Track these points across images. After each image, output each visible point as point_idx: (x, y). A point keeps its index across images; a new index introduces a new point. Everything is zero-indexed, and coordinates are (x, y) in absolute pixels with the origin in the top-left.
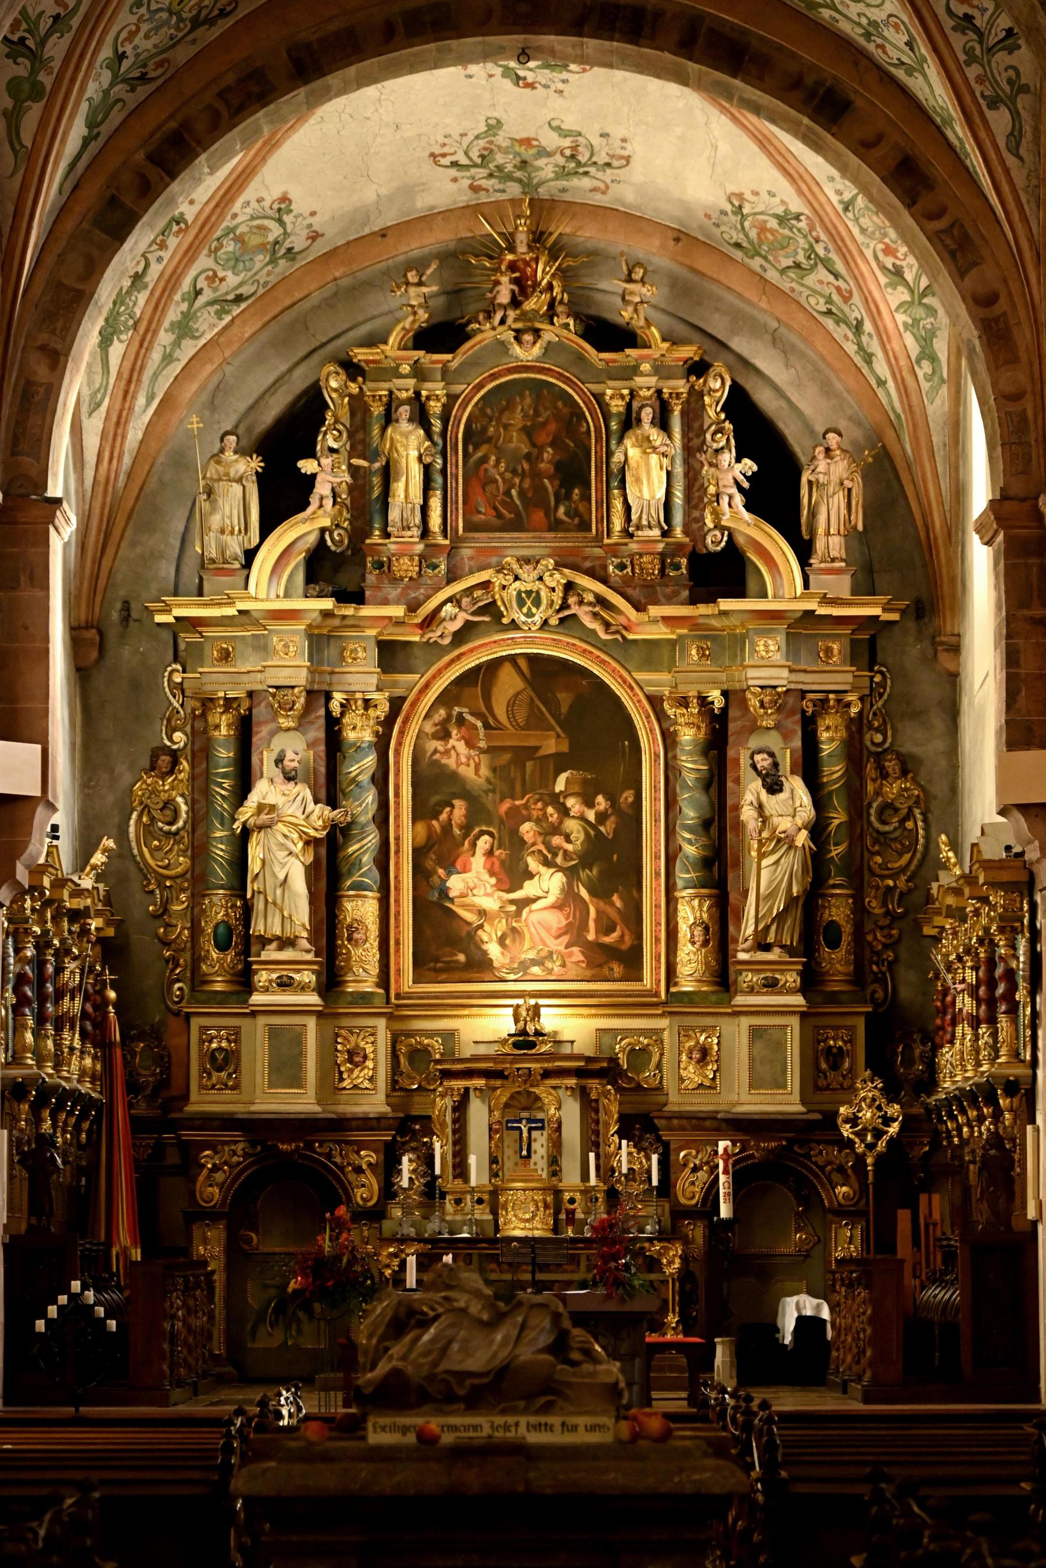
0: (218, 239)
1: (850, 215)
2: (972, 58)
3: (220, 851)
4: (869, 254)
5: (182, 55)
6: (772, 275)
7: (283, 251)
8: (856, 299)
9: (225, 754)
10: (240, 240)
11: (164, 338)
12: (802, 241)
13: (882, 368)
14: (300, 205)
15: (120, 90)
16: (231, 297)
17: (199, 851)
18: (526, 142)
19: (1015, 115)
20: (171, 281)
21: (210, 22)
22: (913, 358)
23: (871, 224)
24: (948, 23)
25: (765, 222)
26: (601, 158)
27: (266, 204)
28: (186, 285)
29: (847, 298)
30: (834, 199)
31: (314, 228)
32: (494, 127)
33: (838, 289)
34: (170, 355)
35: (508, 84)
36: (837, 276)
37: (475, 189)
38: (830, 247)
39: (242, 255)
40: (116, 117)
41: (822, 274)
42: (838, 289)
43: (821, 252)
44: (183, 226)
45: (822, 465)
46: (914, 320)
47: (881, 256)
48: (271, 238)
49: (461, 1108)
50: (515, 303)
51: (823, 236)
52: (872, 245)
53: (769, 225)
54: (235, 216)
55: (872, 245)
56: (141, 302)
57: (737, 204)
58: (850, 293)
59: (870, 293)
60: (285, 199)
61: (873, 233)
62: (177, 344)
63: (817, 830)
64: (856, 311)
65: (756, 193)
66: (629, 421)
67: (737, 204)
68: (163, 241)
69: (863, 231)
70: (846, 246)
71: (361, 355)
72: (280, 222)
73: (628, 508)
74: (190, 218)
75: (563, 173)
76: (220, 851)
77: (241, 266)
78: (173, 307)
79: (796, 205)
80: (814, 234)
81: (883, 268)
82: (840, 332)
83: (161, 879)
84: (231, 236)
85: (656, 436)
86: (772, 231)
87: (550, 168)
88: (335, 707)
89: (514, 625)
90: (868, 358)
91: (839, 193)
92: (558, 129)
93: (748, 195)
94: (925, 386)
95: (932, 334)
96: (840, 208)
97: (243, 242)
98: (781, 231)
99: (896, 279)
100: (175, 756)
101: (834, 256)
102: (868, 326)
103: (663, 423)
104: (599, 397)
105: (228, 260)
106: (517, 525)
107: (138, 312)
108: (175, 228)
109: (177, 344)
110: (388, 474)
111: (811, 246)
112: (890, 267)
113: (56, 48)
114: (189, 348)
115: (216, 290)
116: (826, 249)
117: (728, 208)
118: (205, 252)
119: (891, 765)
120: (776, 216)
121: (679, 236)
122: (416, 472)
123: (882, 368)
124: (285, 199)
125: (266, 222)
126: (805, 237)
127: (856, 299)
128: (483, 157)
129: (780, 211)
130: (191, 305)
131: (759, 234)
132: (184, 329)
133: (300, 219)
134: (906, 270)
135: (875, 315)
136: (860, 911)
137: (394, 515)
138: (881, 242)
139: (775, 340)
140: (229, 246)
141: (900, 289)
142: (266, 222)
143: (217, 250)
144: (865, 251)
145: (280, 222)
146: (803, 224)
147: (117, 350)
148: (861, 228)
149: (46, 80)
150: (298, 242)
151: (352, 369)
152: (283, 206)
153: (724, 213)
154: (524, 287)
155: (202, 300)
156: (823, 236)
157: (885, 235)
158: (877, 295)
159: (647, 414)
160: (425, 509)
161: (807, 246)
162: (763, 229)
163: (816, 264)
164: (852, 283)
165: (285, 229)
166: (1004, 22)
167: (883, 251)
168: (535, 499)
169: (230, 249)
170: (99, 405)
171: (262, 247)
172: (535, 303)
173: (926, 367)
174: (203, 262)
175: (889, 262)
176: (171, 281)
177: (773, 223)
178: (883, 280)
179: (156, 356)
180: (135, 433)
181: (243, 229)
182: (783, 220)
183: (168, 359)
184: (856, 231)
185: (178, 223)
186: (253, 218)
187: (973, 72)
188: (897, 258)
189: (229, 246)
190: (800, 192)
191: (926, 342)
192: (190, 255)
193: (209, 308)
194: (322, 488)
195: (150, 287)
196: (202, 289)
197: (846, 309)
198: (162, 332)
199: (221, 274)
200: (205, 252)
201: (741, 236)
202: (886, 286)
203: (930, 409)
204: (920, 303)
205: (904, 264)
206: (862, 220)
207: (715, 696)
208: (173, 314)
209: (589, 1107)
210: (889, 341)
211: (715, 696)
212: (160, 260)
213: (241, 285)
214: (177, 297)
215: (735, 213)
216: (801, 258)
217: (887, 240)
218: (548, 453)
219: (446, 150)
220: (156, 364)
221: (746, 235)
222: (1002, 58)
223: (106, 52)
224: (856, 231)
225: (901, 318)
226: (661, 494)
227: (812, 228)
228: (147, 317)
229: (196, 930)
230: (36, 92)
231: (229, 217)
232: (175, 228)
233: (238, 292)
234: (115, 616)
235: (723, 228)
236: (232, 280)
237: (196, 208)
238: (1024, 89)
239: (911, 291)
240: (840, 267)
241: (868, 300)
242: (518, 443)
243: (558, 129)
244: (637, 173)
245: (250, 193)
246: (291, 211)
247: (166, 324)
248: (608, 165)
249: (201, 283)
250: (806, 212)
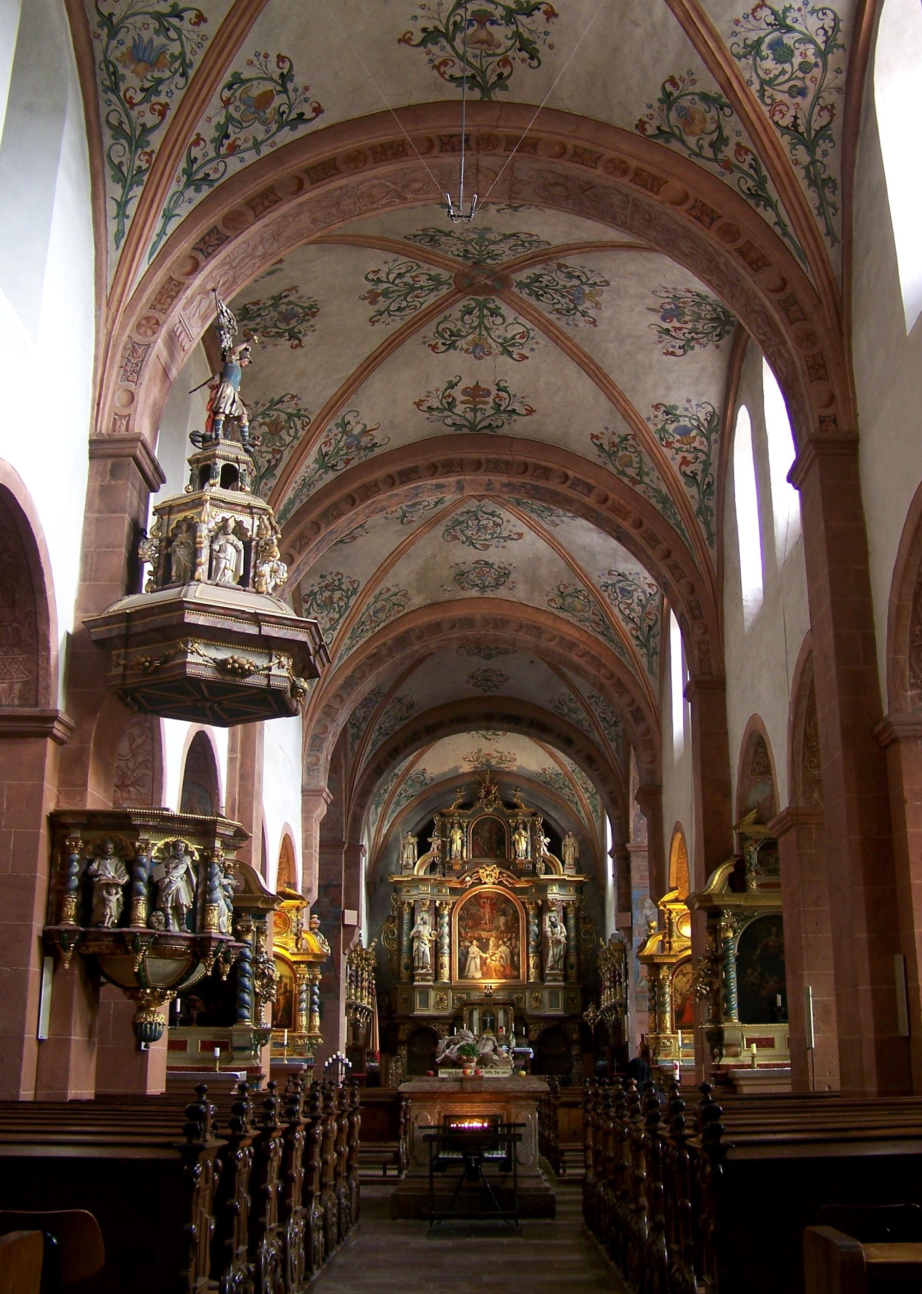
2: (606, 729)
3: (405, 943)
5: (397, 728)
6: (553, 790)
9: (406, 917)
10: (413, 780)
11: (392, 806)
13: (583, 815)
14: (429, 771)
15: (381, 737)
17: (400, 943)
18: (488, 755)
19: (617, 744)
20: (394, 792)
21: (405, 719)
24: (599, 719)
28: (398, 792)
29: (573, 796)
32: (480, 751)
40: (380, 744)
45: (567, 840)
49: (471, 1014)
50: (486, 797)
62: (395, 808)
63: (567, 938)
64: (576, 799)
66: (516, 828)
71: (444, 810)
73: (516, 851)
75: (498, 763)
76: (405, 943)
79: (560, 771)
82: (571, 805)
83: (390, 951)
85: (523, 833)
88: (437, 904)
89: (485, 883)
90: (579, 812)
100: (394, 918)
103: (525, 830)
104: (508, 822)
106: (486, 856)
109: (395, 808)
110: (452, 842)
113: (364, 726)
114: (399, 809)
119: (587, 920)
121: (529, 780)
122: (459, 842)
123: (583, 815)
132: (398, 804)
135: (581, 800)
136: (578, 959)
137: (453, 853)
139: (554, 807)
140: (410, 782)
147: (380, 809)
149: (361, 734)
150: (428, 781)
151: (442, 815)
154: (488, 792)
159: (521, 826)
160: (462, 852)
162: (551, 778)
166: (614, 719)
168: (491, 850)
172: (491, 797)
174: (403, 786)
179: (390, 811)
180: (384, 831)
183: (393, 812)
187: (606, 732)
189: (410, 782)
191: (594, 807)
192: (399, 784)
194: (434, 846)
207: (540, 902)
208: (395, 800)
209: (506, 1013)
211: (540, 902)
218: (494, 837)
222: (613, 729)
223: (377, 727)
226: (524, 848)
229: (399, 965)
230: (358, 737)
234: (378, 880)
236: (410, 791)
238: (619, 737)
241: (579, 796)
242: (486, 834)
244: (518, 763)
245: (415, 768)
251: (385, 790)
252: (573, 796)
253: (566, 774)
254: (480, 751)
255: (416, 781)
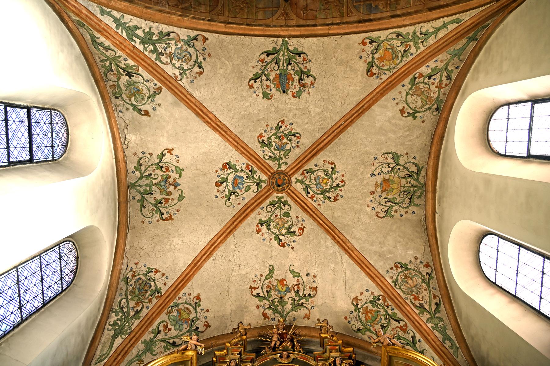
0: (172, 307)
1: (397, 287)
4: (408, 302)
7: (194, 328)
8: (410, 326)
10: (179, 311)
12: (382, 311)
16: (171, 341)
18: (282, 282)
20: (150, 320)
22: (441, 340)
23: (406, 288)
25: (367, 307)
26: (307, 292)
27: (192, 297)
29: (404, 329)
30: (390, 281)
31: (208, 320)
33: (401, 328)
34: (140, 356)
35: (276, 243)
36: (398, 321)
37: (265, 316)
38: (394, 307)
39: (179, 320)
41: (394, 324)
42: (401, 328)
43: (390, 312)
44: (160, 294)
46: (435, 324)
47: (413, 301)
48: (191, 318)
51: (390, 303)
52: (409, 297)
53: (369, 308)
54: (179, 298)
55: (409, 297)
56: (136, 324)
57: (355, 304)
58: (406, 325)
59: (414, 318)
60: (198, 297)
61: (408, 292)
65: (362, 294)
67: (355, 304)
68: (151, 299)
69: (404, 292)
70: (399, 301)
72: (195, 309)
74: (163, 292)
77: (177, 326)
78: (147, 333)
79: (377, 292)
80: (386, 303)
81: (416, 306)
84: (177, 308)
86: (370, 312)
87: (290, 302)
91: (391, 278)
92: (292, 271)
93: (360, 297)
94: (451, 351)
95: (445, 328)
96: (393, 285)
97: (180, 313)
98: (374, 309)
99: (422, 310)
101: (396, 311)
102: (418, 337)
105: (173, 320)
107: (133, 328)
108: (157, 295)
111: (386, 311)
112: (418, 305)
115: (166, 334)
116: (392, 309)
117: (353, 308)
118: (165, 311)
120: (371, 302)
124: (198, 297)
125: (190, 308)
126: (383, 308)
127: (410, 326)
128: (267, 292)
129: (371, 299)
130: (155, 337)
131: (365, 317)
133: (203, 312)
134: (424, 304)
138: (412, 295)
141: (425, 313)
142: (190, 308)
143: (171, 312)
144: (406, 301)
145: (195, 309)
146: (381, 302)
148: (403, 291)
152: (197, 301)
153: (351, 313)
155: (160, 337)
156: (390, 303)
157: (412, 291)
158: (417, 318)
161: (384, 313)
162: (367, 312)
163: (390, 321)
164: (405, 320)
165: (197, 315)
167: (413, 298)
169: (175, 314)
170: (102, 361)
171: (186, 321)
173: (448, 344)
175: (417, 303)
176: (150, 320)
177: (370, 307)
178: (417, 312)
181: (181, 307)
182: (373, 302)
184: (401, 293)
185: (158, 293)
186: (186, 303)
188: (420, 300)
189: (175, 314)
190: (377, 284)
191: (443, 332)
193: (162, 343)
195: (141, 319)
196: (160, 331)
197: (406, 336)
198: (140, 342)
199: (170, 326)
200: (165, 311)
201: (360, 323)
202: (419, 313)
203: (458, 360)
204: (435, 317)
205: (423, 302)
206: (402, 287)
208: (147, 336)
210: (429, 335)
212: (148, 307)
213: (176, 337)
214: (150, 329)
215: (355, 310)
216: (383, 321)
217: (414, 293)
219: (255, 285)
220: (133, 356)
221: (361, 321)
224: (401, 293)
225: (429, 325)
227: (385, 301)
228: (136, 331)
231: (177, 298)
232: (157, 295)
233: (175, 340)
235: (352, 323)
236: (173, 333)
237: (166, 288)
239: (430, 313)
240: (400, 315)
243: (292, 271)
245: (185, 290)
246: (200, 305)
247: (142, 339)
248: (309, 295)
249: (161, 328)
250: (382, 294)
251: (137, 312)
252: (404, 329)
253: (388, 294)
254: (271, 271)
255: (185, 315)
